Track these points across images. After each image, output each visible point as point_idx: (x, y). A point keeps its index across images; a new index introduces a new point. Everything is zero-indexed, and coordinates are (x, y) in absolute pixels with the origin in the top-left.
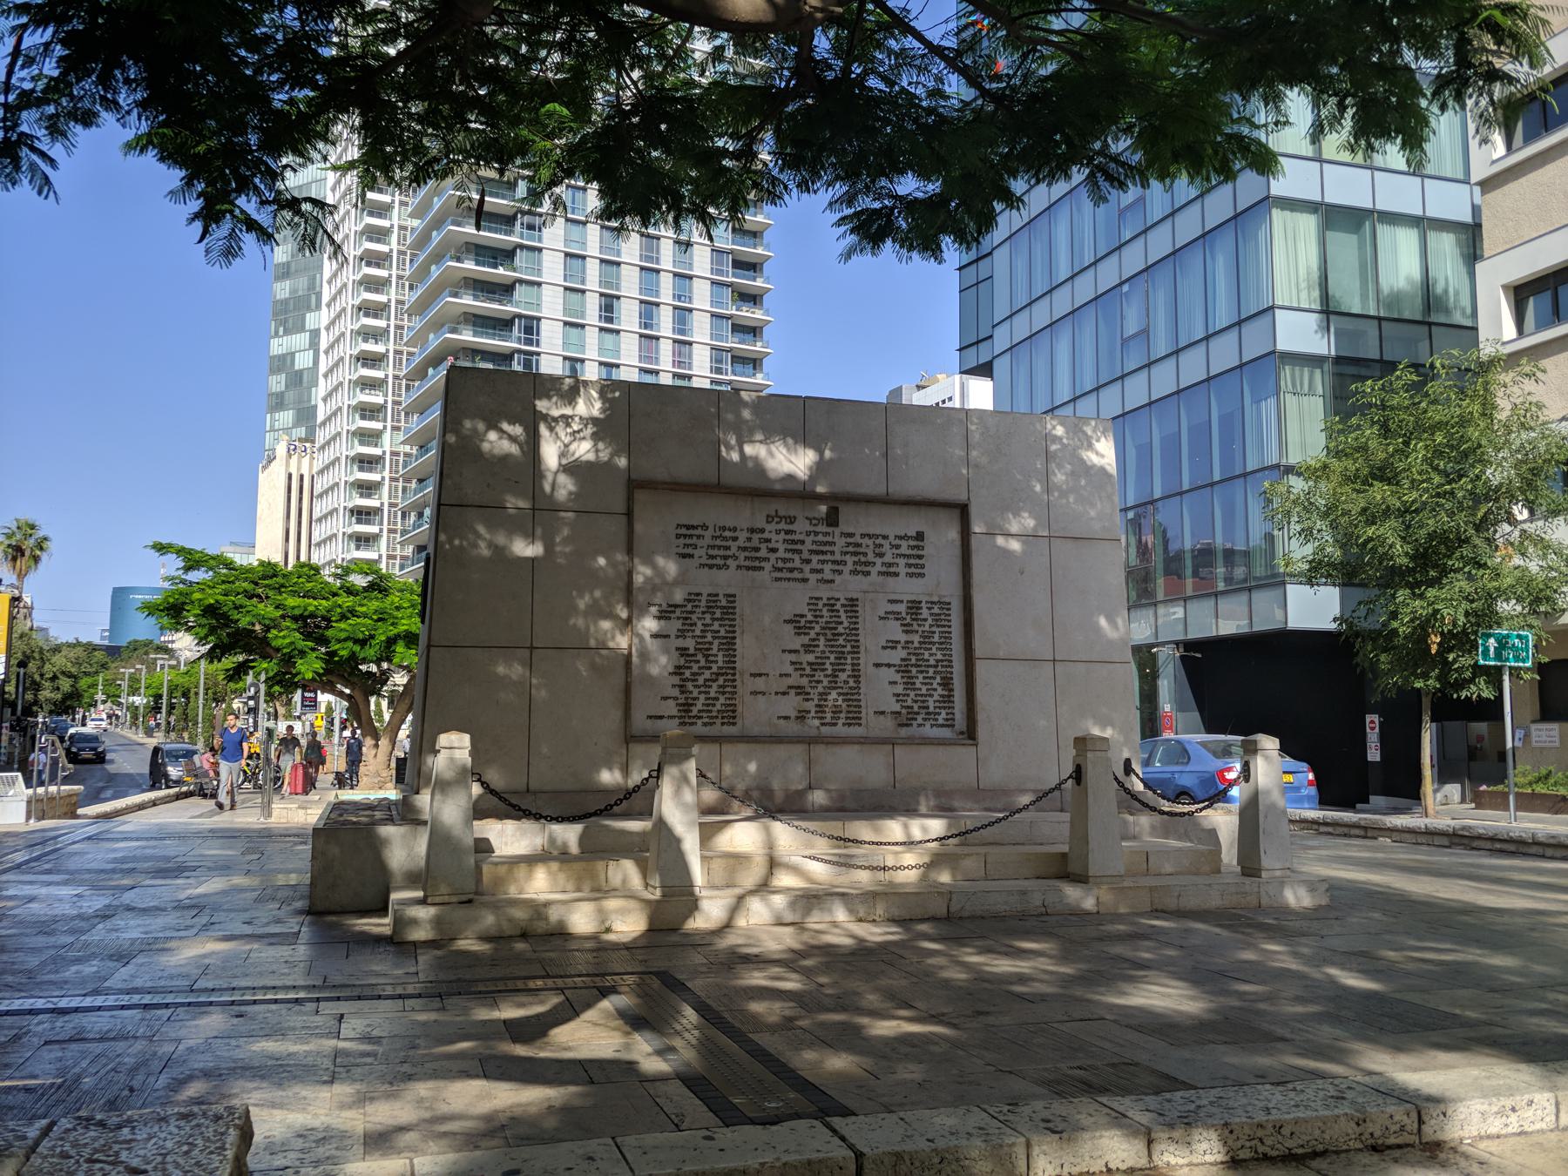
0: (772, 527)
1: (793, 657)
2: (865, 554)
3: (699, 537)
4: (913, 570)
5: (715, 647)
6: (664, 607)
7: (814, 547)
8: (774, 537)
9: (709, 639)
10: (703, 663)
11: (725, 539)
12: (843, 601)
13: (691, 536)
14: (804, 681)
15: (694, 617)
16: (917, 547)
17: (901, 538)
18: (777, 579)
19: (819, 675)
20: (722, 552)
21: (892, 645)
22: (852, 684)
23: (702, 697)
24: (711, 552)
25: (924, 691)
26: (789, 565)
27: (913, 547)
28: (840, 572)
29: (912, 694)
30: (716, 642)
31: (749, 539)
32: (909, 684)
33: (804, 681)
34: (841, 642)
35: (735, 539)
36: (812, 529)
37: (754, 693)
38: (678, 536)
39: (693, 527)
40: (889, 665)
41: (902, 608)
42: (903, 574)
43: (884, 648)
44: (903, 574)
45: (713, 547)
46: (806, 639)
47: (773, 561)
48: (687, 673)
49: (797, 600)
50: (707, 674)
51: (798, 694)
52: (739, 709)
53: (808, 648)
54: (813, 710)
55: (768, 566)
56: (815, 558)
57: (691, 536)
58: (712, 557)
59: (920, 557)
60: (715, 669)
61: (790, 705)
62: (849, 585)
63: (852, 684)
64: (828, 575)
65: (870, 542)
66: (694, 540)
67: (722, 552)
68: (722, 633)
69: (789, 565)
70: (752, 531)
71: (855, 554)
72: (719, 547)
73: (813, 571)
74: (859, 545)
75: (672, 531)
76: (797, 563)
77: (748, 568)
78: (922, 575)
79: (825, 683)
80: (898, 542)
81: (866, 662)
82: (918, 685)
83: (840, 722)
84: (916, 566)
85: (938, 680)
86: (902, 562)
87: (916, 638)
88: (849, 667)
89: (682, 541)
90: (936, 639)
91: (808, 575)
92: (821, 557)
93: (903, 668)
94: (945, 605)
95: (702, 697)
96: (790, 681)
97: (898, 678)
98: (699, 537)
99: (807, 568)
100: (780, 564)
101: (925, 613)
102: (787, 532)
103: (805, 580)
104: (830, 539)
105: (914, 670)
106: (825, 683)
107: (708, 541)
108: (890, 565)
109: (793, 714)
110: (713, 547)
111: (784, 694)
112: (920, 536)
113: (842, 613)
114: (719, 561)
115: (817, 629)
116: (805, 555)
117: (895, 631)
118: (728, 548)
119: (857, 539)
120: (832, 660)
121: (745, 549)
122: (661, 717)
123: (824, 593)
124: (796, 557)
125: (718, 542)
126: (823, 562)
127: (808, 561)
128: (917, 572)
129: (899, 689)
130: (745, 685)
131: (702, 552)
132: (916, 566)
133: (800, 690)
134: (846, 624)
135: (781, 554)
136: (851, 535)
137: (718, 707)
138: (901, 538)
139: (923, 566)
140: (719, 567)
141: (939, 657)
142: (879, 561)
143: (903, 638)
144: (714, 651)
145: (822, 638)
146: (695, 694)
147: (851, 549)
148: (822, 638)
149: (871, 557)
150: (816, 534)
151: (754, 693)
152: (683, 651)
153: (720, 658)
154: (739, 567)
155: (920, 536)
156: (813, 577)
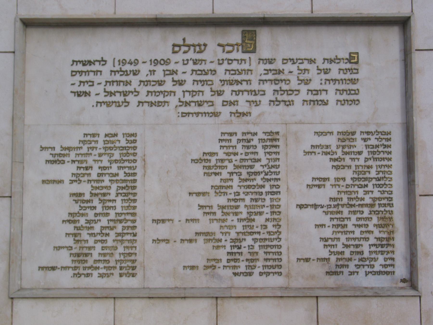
3: (96, 72)
5: (113, 191)
15: (90, 160)
18: (185, 115)
20: (121, 88)
24: (110, 88)
34: (259, 180)
37: (157, 241)
55: (173, 101)
61: (199, 253)
67: (121, 88)
77: (151, 104)
79: (239, 228)
88: (267, 210)
95: (99, 246)
107: (106, 76)
114: (119, 98)
118: (128, 83)
122: (53, 268)
126: (237, 93)
137: (117, 257)
141: (377, 194)
145: (236, 178)
147: (270, 76)
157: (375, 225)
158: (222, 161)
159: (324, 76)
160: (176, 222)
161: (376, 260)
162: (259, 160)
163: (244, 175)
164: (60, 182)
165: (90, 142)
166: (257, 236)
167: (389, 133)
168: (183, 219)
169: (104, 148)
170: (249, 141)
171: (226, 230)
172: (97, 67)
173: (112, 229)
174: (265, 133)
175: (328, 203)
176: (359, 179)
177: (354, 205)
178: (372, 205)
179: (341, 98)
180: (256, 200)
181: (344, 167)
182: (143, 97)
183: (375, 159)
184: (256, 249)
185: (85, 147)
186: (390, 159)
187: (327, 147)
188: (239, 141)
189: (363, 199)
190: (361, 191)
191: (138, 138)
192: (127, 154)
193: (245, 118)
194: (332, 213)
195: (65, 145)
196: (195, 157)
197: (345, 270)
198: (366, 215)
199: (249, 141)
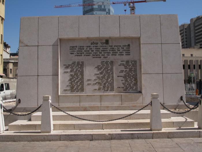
0: (92, 45)
1: (98, 76)
2: (115, 50)
3: (75, 49)
4: (127, 53)
5: (79, 74)
6: (67, 65)
8: (93, 48)
9: (77, 72)
10: (76, 78)
11: (81, 49)
12: (110, 62)
13: (73, 49)
14: (100, 81)
15: (74, 67)
16: (128, 48)
17: (124, 46)
18: (94, 58)
19: (104, 79)
20: (80, 52)
21: (122, 71)
22: (112, 81)
23: (76, 85)
25: (130, 82)
26: (96, 54)
27: (127, 48)
28: (109, 55)
29: (127, 83)
30: (79, 73)
31: (87, 49)
32: (126, 80)
33: (100, 81)
34: (109, 71)
35: (83, 49)
36: (102, 45)
38: (70, 49)
39: (74, 47)
40: (121, 76)
41: (124, 63)
42: (124, 55)
43: (120, 72)
44: (124, 55)
45: (78, 51)
46: (101, 71)
47: (93, 53)
48: (73, 80)
50: (77, 80)
51: (99, 84)
53: (101, 73)
55: (91, 55)
56: (103, 52)
57: (73, 49)
58: (78, 53)
59: (129, 50)
62: (111, 58)
63: (112, 81)
64: (106, 56)
65: (117, 48)
66: (74, 50)
67: (80, 52)
69: (96, 54)
70: (88, 47)
71: (113, 50)
72: (80, 51)
73: (102, 55)
74: (113, 48)
75: (69, 48)
76: (98, 54)
78: (129, 55)
82: (128, 81)
84: (128, 52)
85: (133, 79)
86: (124, 52)
87: (128, 70)
89: (71, 50)
90: (133, 69)
92: (104, 52)
93: (125, 77)
94: (135, 62)
95: (76, 85)
96: (97, 81)
97: (123, 79)
98: (75, 49)
99: (101, 55)
100: (94, 54)
101: (130, 64)
102: (96, 47)
103: (100, 57)
104: (106, 47)
105: (127, 77)
107: (77, 50)
108: (121, 53)
110: (78, 51)
112: (129, 45)
114: (80, 54)
117: (123, 68)
118: (82, 51)
119: (113, 47)
120: (107, 76)
121: (85, 51)
123: (105, 60)
124: (98, 52)
125: (80, 50)
126: (105, 53)
127: (101, 53)
128: (128, 54)
129: (124, 82)
130: (86, 83)
131: (76, 52)
132: (128, 52)
133: (99, 83)
135: (94, 52)
136: (112, 46)
138: (124, 46)
139: (130, 53)
140: (80, 56)
141: (134, 74)
142: (118, 52)
143: (125, 70)
145: (104, 71)
147: (111, 49)
148: (104, 71)
149: (116, 51)
152: (71, 75)
153: (80, 76)
154: (84, 55)
155: (129, 45)
156: (102, 57)
157: (134, 80)
158: (102, 67)
159: (122, 49)
161: (134, 87)
162: (109, 67)
164: (68, 72)
165: (74, 64)
167: (136, 61)
168: (94, 80)
169: (77, 65)
170: (107, 63)
172: (75, 48)
174: (111, 61)
176: (130, 71)
177: (129, 76)
180: (109, 75)
181: (127, 68)
182: (85, 54)
184: (109, 85)
185: (73, 65)
186: (136, 66)
187: (124, 64)
188: (105, 63)
189: (131, 75)
190: (131, 73)
191: (84, 63)
192: (82, 66)
193: (106, 58)
195: (69, 64)
196: (96, 66)
197: (127, 90)
199: (107, 63)
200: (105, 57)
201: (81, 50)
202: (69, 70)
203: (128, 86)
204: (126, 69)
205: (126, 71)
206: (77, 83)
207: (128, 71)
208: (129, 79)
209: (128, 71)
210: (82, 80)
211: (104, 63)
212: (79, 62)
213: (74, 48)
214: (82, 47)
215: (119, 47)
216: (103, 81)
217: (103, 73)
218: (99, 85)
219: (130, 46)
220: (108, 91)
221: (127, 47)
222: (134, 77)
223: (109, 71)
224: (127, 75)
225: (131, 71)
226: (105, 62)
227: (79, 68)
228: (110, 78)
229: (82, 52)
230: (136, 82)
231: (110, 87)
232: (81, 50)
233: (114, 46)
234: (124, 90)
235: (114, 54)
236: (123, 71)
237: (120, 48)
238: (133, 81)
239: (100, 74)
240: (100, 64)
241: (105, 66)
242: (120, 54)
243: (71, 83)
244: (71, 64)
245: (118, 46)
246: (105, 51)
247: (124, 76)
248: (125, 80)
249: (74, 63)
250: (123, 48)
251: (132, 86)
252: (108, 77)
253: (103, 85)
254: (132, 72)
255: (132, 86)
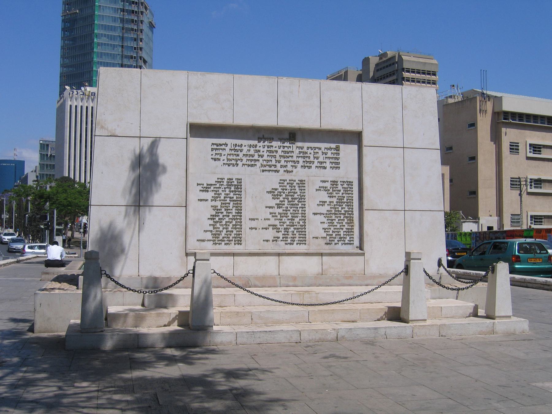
1: (271, 210)
4: (334, 165)
6: (205, 185)
7: (283, 154)
10: (225, 213)
12: (297, 181)
15: (220, 190)
18: (263, 171)
20: (235, 157)
21: (323, 203)
22: (301, 223)
25: (338, 227)
29: (332, 228)
31: (249, 150)
32: (331, 223)
33: (277, 223)
34: (296, 202)
35: (241, 151)
37: (251, 228)
40: (321, 214)
41: (328, 185)
42: (328, 168)
45: (230, 155)
46: (278, 201)
49: (272, 180)
50: (227, 219)
51: (273, 229)
52: (243, 236)
53: (279, 206)
54: (281, 236)
55: (258, 164)
56: (283, 160)
60: (231, 217)
62: (299, 173)
63: (301, 223)
64: (289, 168)
65: (312, 152)
67: (235, 157)
68: (235, 198)
71: (304, 157)
73: (281, 166)
75: (210, 148)
77: (249, 165)
79: (288, 223)
80: (326, 151)
81: (309, 212)
82: (335, 224)
83: (295, 243)
85: (346, 221)
86: (328, 161)
87: (335, 200)
88: (300, 215)
90: (345, 200)
91: (278, 168)
92: (286, 159)
93: (328, 215)
94: (350, 183)
95: (225, 231)
97: (325, 220)
99: (278, 165)
100: (265, 163)
101: (340, 187)
103: (278, 171)
104: (291, 150)
106: (288, 223)
107: (228, 151)
108: (321, 163)
109: (271, 239)
110: (230, 155)
111: (266, 229)
113: (297, 188)
115: (284, 196)
116: (278, 158)
118: (238, 155)
119: (305, 150)
120: (291, 211)
123: (288, 177)
124: (273, 160)
127: (279, 162)
128: (336, 166)
129: (326, 226)
130: (246, 224)
131: (225, 158)
133: (274, 226)
134: (299, 193)
135: (265, 158)
136: (302, 148)
137: (233, 235)
142: (316, 161)
144: (231, 208)
146: (221, 229)
148: (286, 200)
149: (312, 159)
150: (284, 147)
151: (251, 228)
152: (215, 208)
153: (234, 211)
156: (282, 170)
157: (346, 223)
158: (280, 192)
160: (260, 220)
163: (290, 199)
164: (207, 200)
165: (220, 182)
166: (295, 227)
167: (352, 182)
171: (282, 224)
172: (223, 147)
173: (231, 222)
175: (326, 212)
176: (340, 202)
178: (344, 214)
179: (332, 166)
181: (333, 197)
182: (244, 162)
183: (346, 194)
184: (295, 232)
192: (238, 188)
194: (328, 217)
197: (333, 243)
198: (342, 218)
200: (287, 171)
201: (236, 153)
202: (209, 195)
203: (334, 235)
204: (331, 200)
205: (330, 202)
206: (226, 225)
207: (335, 203)
208: (337, 220)
209: (335, 203)
210: (237, 219)
211: (286, 184)
212: (232, 179)
213: (221, 147)
214: (239, 146)
215: (317, 150)
216: (284, 223)
217: (284, 204)
218: (275, 230)
219: (339, 150)
220: (293, 244)
221: (333, 151)
222: (347, 217)
223: (296, 202)
224: (333, 212)
225: (342, 202)
226: (288, 181)
227: (233, 191)
228: (297, 217)
229: (238, 158)
230: (350, 227)
231: (297, 236)
232: (236, 153)
233: (308, 148)
234: (327, 244)
235: (306, 165)
236: (325, 202)
237: (320, 152)
238: (344, 224)
239: (276, 207)
240: (277, 186)
241: (287, 191)
242: (319, 165)
243: (213, 225)
244: (214, 183)
245: (315, 148)
246: (288, 157)
247: (327, 214)
248: (329, 221)
249: (220, 180)
250: (326, 154)
251: (342, 236)
252: (294, 214)
253: (283, 232)
254: (344, 206)
255: (342, 236)
